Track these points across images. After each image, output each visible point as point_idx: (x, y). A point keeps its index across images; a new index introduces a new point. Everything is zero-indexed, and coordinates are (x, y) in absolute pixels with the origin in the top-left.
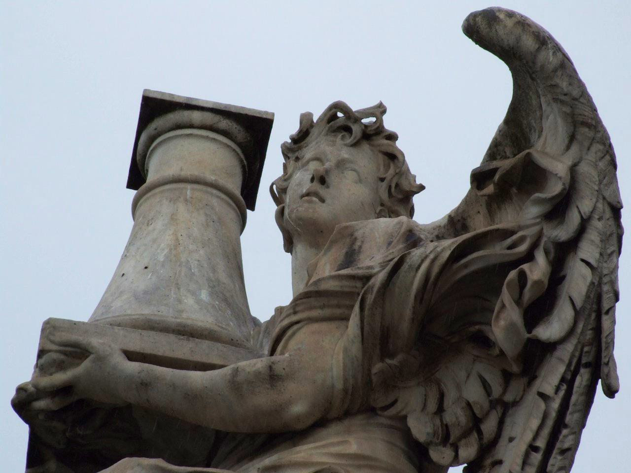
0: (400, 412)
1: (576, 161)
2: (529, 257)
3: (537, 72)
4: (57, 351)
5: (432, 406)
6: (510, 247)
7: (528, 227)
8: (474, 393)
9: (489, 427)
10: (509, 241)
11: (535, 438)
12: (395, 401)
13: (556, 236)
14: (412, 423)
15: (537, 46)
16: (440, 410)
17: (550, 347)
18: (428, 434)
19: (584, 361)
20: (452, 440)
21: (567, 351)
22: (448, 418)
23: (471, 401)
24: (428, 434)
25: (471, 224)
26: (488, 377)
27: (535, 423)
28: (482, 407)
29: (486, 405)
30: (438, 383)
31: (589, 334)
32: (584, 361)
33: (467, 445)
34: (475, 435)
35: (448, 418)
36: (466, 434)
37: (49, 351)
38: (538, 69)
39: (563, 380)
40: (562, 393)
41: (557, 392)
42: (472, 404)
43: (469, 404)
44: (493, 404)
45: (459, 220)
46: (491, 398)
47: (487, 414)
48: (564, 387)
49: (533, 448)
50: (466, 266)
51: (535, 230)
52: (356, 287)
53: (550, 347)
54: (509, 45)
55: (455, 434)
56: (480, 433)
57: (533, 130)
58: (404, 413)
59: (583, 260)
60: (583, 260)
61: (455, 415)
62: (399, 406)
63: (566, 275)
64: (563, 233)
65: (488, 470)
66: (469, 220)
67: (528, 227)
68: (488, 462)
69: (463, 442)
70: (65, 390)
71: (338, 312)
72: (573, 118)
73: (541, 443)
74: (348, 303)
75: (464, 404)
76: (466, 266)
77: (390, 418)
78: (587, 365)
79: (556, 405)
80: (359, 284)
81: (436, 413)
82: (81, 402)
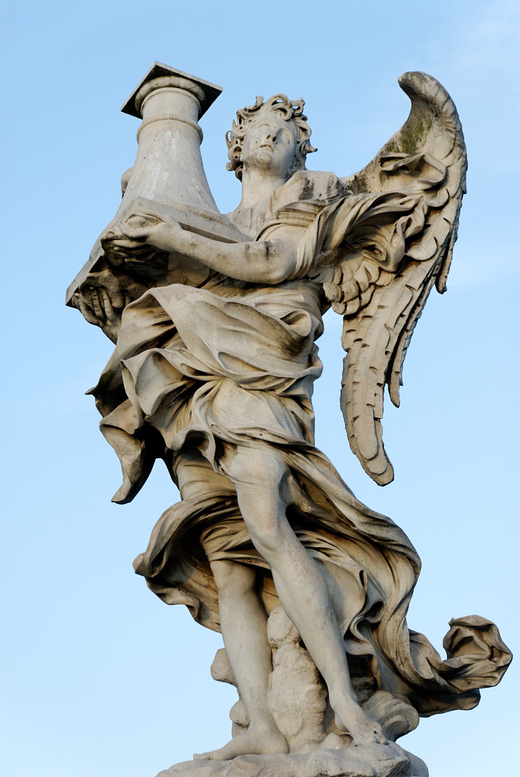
0: (320, 281)
1: (450, 164)
2: (411, 211)
3: (442, 113)
4: (142, 216)
5: (337, 280)
6: (401, 204)
7: (414, 194)
8: (361, 278)
9: (366, 297)
10: (402, 200)
12: (319, 275)
13: (432, 203)
14: (325, 287)
15: (446, 100)
16: (341, 283)
18: (334, 295)
20: (344, 301)
21: (427, 267)
23: (359, 282)
24: (334, 295)
25: (368, 183)
26: (370, 270)
28: (365, 286)
29: (367, 285)
31: (441, 259)
32: (434, 273)
33: (352, 304)
34: (358, 299)
36: (353, 299)
38: (444, 112)
42: (360, 283)
43: (357, 283)
44: (370, 284)
45: (360, 180)
46: (370, 282)
47: (366, 290)
48: (423, 285)
49: (401, 315)
50: (377, 210)
52: (315, 211)
54: (430, 96)
56: (360, 299)
57: (419, 140)
58: (321, 282)
59: (444, 219)
60: (444, 219)
61: (349, 287)
62: (320, 278)
64: (436, 203)
65: (360, 320)
66: (367, 180)
67: (414, 194)
68: (361, 315)
69: (351, 302)
70: (142, 239)
71: (302, 222)
72: (455, 141)
73: (407, 313)
74: (312, 219)
75: (355, 283)
76: (377, 210)
77: (315, 283)
78: (434, 275)
79: (417, 294)
80: (317, 209)
81: (338, 285)
82: (148, 246)
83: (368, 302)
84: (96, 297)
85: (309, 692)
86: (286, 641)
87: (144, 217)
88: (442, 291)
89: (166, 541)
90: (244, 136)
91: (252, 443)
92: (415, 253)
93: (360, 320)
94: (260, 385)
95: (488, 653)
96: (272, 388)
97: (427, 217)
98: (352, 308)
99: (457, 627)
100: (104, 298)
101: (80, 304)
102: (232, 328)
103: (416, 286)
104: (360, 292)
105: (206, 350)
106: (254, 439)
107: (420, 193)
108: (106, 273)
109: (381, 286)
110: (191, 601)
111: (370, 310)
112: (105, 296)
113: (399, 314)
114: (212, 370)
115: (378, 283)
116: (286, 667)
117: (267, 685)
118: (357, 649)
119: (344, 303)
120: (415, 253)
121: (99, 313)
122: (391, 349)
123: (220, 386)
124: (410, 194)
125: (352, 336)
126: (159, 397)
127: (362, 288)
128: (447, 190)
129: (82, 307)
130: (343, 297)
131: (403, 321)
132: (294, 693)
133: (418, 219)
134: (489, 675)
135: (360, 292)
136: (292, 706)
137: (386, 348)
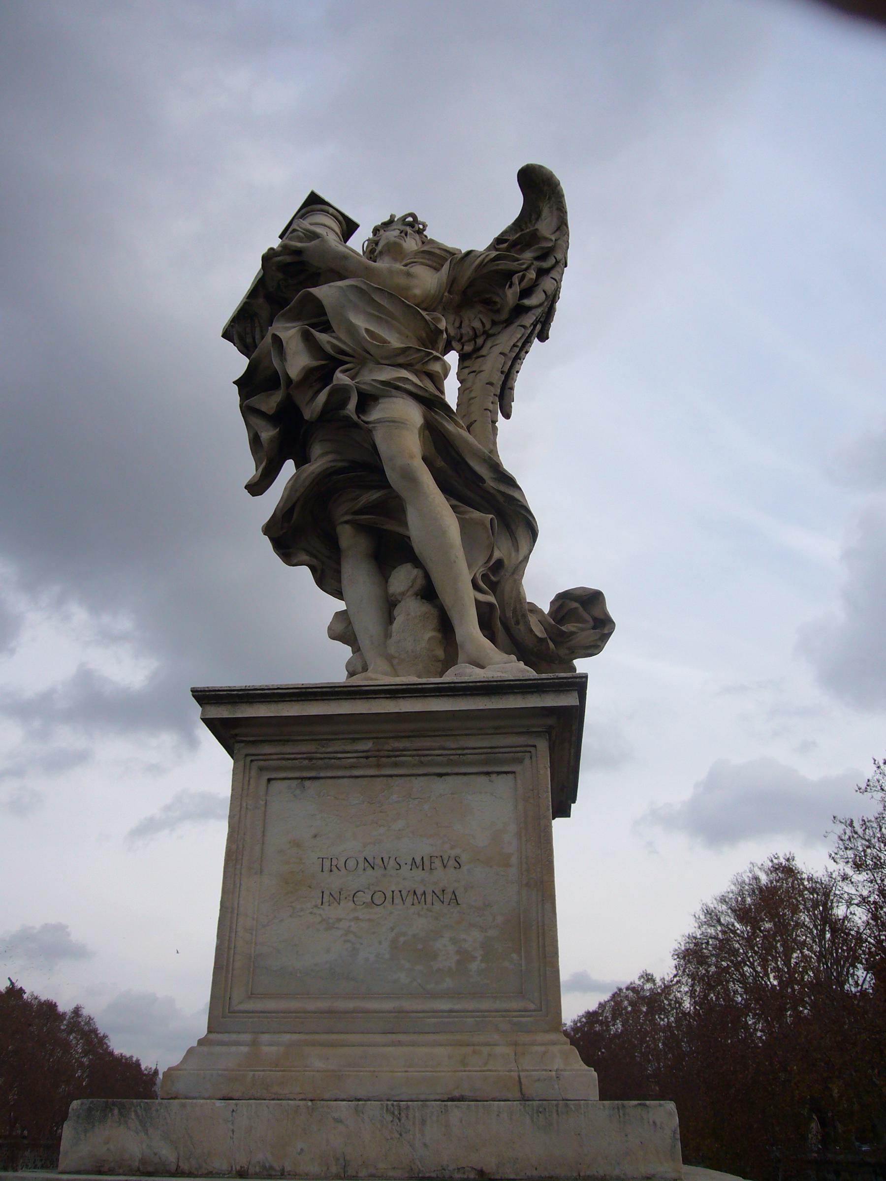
4: (301, 232)
5: (457, 324)
8: (477, 325)
9: (480, 341)
11: (517, 341)
16: (460, 327)
17: (529, 309)
19: (541, 320)
20: (462, 341)
22: (463, 331)
26: (485, 321)
27: (519, 336)
29: (482, 331)
30: (461, 317)
34: (474, 342)
35: (463, 331)
36: (469, 341)
37: (298, 231)
39: (532, 324)
40: (532, 328)
41: (530, 327)
44: (485, 332)
46: (484, 329)
47: (480, 336)
49: (514, 346)
51: (530, 262)
53: (529, 309)
55: (465, 338)
56: (475, 343)
61: (466, 330)
63: (540, 283)
64: (546, 265)
69: (467, 343)
70: (298, 252)
71: (435, 264)
73: (520, 344)
76: (498, 265)
78: (541, 322)
81: (458, 328)
82: (302, 263)
83: (481, 345)
84: (249, 325)
85: (429, 639)
86: (408, 594)
87: (303, 233)
88: (507, 416)
89: (298, 494)
90: (379, 240)
91: (394, 392)
92: (527, 302)
93: (474, 359)
94: (401, 360)
95: (592, 623)
96: (411, 361)
97: (538, 276)
98: (468, 348)
99: (563, 600)
100: (256, 325)
101: (234, 333)
102: (377, 313)
103: (528, 325)
104: (476, 336)
105: (352, 330)
106: (397, 388)
107: (531, 260)
108: (261, 300)
109: (494, 335)
110: (314, 562)
111: (484, 352)
112: (257, 324)
113: (512, 344)
114: (354, 350)
115: (491, 332)
116: (408, 615)
117: (387, 635)
118: (481, 597)
119: (462, 343)
120: (527, 302)
121: (249, 340)
122: (506, 369)
123: (360, 369)
124: (523, 259)
125: (467, 371)
126: (304, 368)
127: (478, 334)
128: (555, 257)
129: (235, 337)
130: (461, 338)
131: (517, 350)
132: (414, 641)
133: (532, 274)
134: (592, 644)
135: (476, 336)
136: (412, 652)
137: (502, 368)
